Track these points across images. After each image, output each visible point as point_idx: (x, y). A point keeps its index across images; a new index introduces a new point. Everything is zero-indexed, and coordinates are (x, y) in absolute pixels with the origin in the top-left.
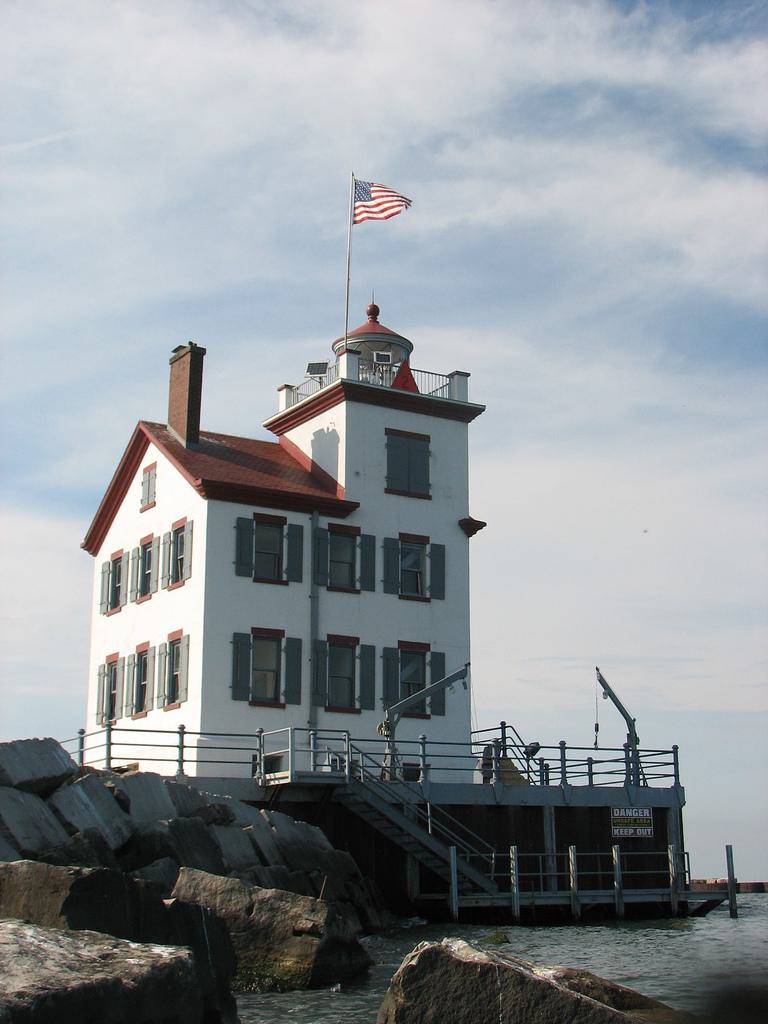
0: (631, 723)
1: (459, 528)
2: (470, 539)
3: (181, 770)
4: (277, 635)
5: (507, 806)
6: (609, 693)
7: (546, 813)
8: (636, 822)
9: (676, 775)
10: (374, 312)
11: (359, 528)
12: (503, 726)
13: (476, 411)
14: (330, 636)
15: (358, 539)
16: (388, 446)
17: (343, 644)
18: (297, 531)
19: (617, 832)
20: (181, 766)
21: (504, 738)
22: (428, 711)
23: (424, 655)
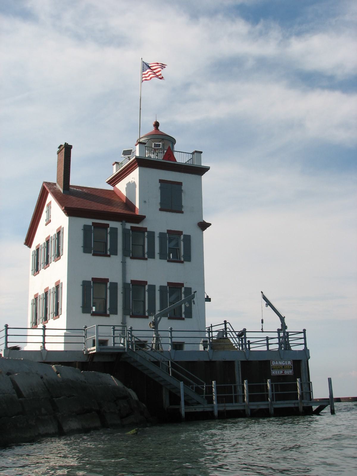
0: (282, 319)
1: (198, 226)
2: (204, 231)
3: (44, 347)
4: (105, 281)
5: (214, 362)
6: (269, 303)
7: (236, 364)
8: (284, 367)
9: (305, 344)
10: (157, 125)
11: (146, 228)
12: (225, 322)
13: (206, 169)
14: (132, 281)
15: (146, 233)
16: (161, 188)
17: (139, 285)
18: (115, 230)
19: (274, 373)
20: (44, 345)
21: (226, 328)
22: (183, 316)
23: (181, 289)
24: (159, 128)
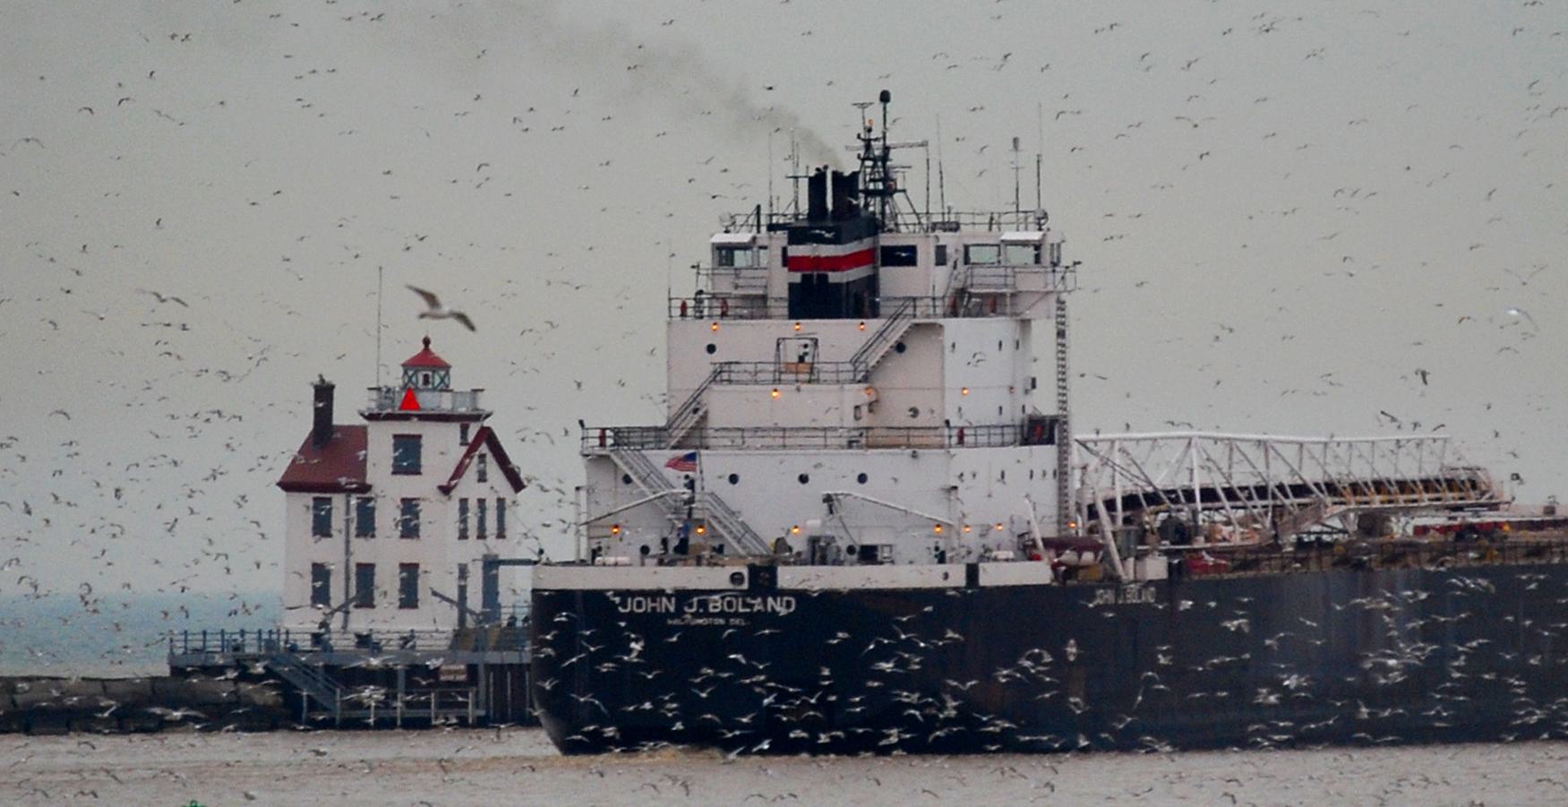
8: (456, 672)
10: (427, 342)
19: (443, 678)
24: (431, 346)
